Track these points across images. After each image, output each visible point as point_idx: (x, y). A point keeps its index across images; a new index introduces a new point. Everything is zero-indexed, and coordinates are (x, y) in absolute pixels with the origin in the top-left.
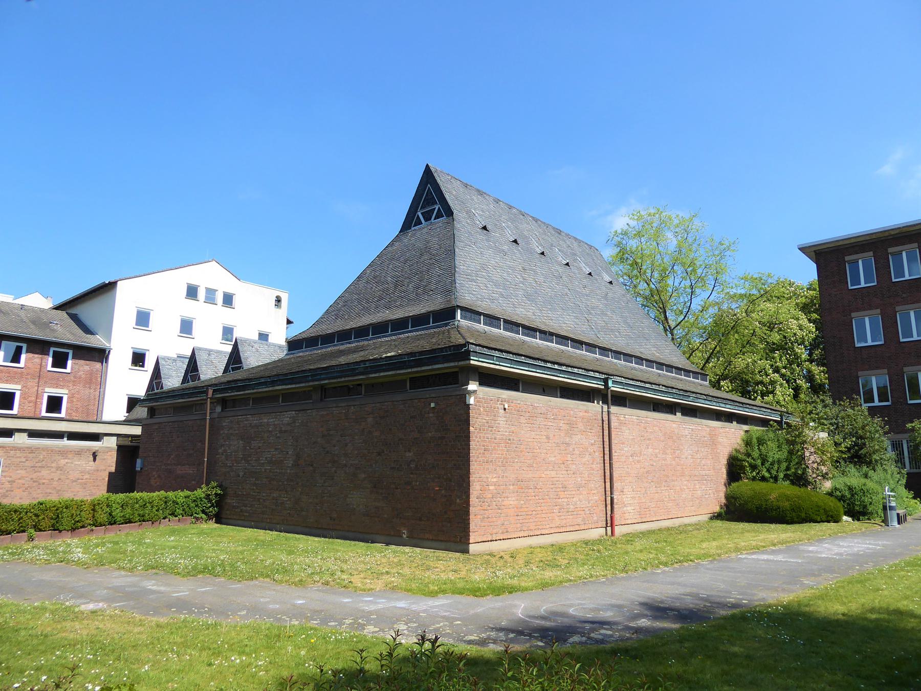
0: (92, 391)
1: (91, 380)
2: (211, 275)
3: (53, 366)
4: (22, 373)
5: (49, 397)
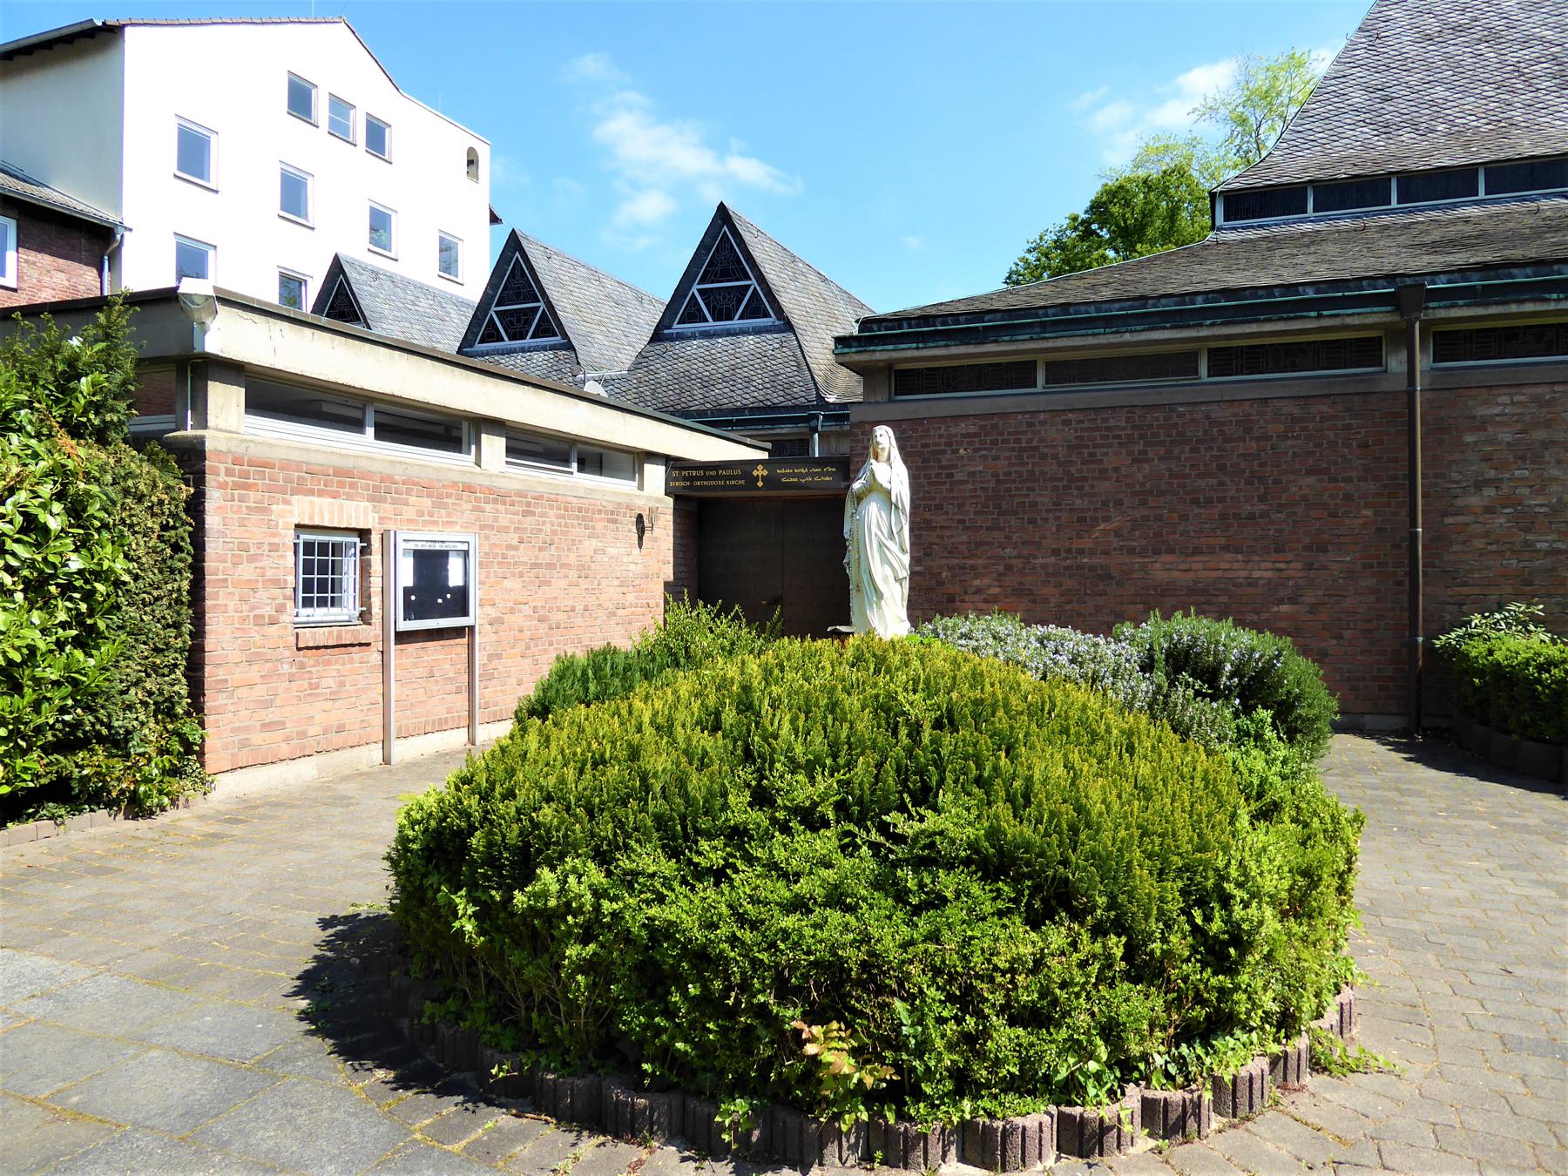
2: (334, 58)
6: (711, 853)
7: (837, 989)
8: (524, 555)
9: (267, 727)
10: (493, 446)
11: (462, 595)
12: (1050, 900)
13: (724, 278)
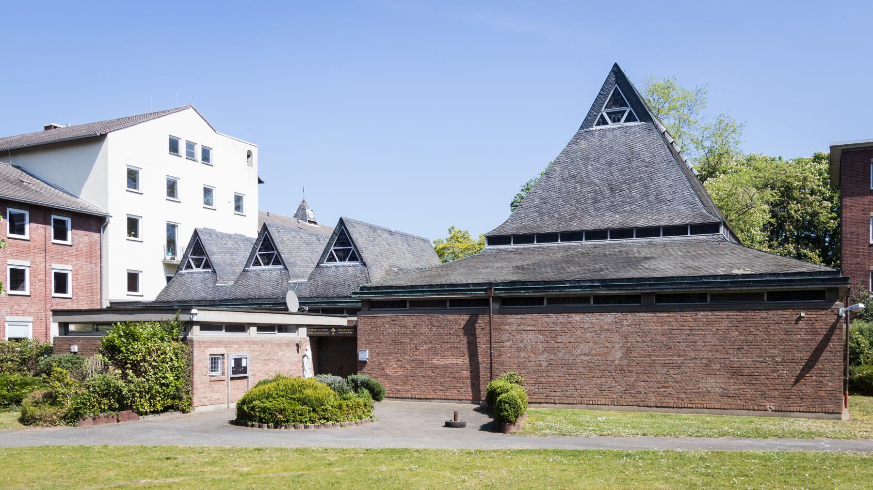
0: (93, 266)
1: (91, 253)
3: (55, 238)
4: (29, 246)
5: (55, 273)
6: (271, 399)
7: (282, 411)
8: (262, 357)
9: (205, 398)
10: (253, 330)
11: (245, 368)
12: (304, 404)
13: (343, 244)
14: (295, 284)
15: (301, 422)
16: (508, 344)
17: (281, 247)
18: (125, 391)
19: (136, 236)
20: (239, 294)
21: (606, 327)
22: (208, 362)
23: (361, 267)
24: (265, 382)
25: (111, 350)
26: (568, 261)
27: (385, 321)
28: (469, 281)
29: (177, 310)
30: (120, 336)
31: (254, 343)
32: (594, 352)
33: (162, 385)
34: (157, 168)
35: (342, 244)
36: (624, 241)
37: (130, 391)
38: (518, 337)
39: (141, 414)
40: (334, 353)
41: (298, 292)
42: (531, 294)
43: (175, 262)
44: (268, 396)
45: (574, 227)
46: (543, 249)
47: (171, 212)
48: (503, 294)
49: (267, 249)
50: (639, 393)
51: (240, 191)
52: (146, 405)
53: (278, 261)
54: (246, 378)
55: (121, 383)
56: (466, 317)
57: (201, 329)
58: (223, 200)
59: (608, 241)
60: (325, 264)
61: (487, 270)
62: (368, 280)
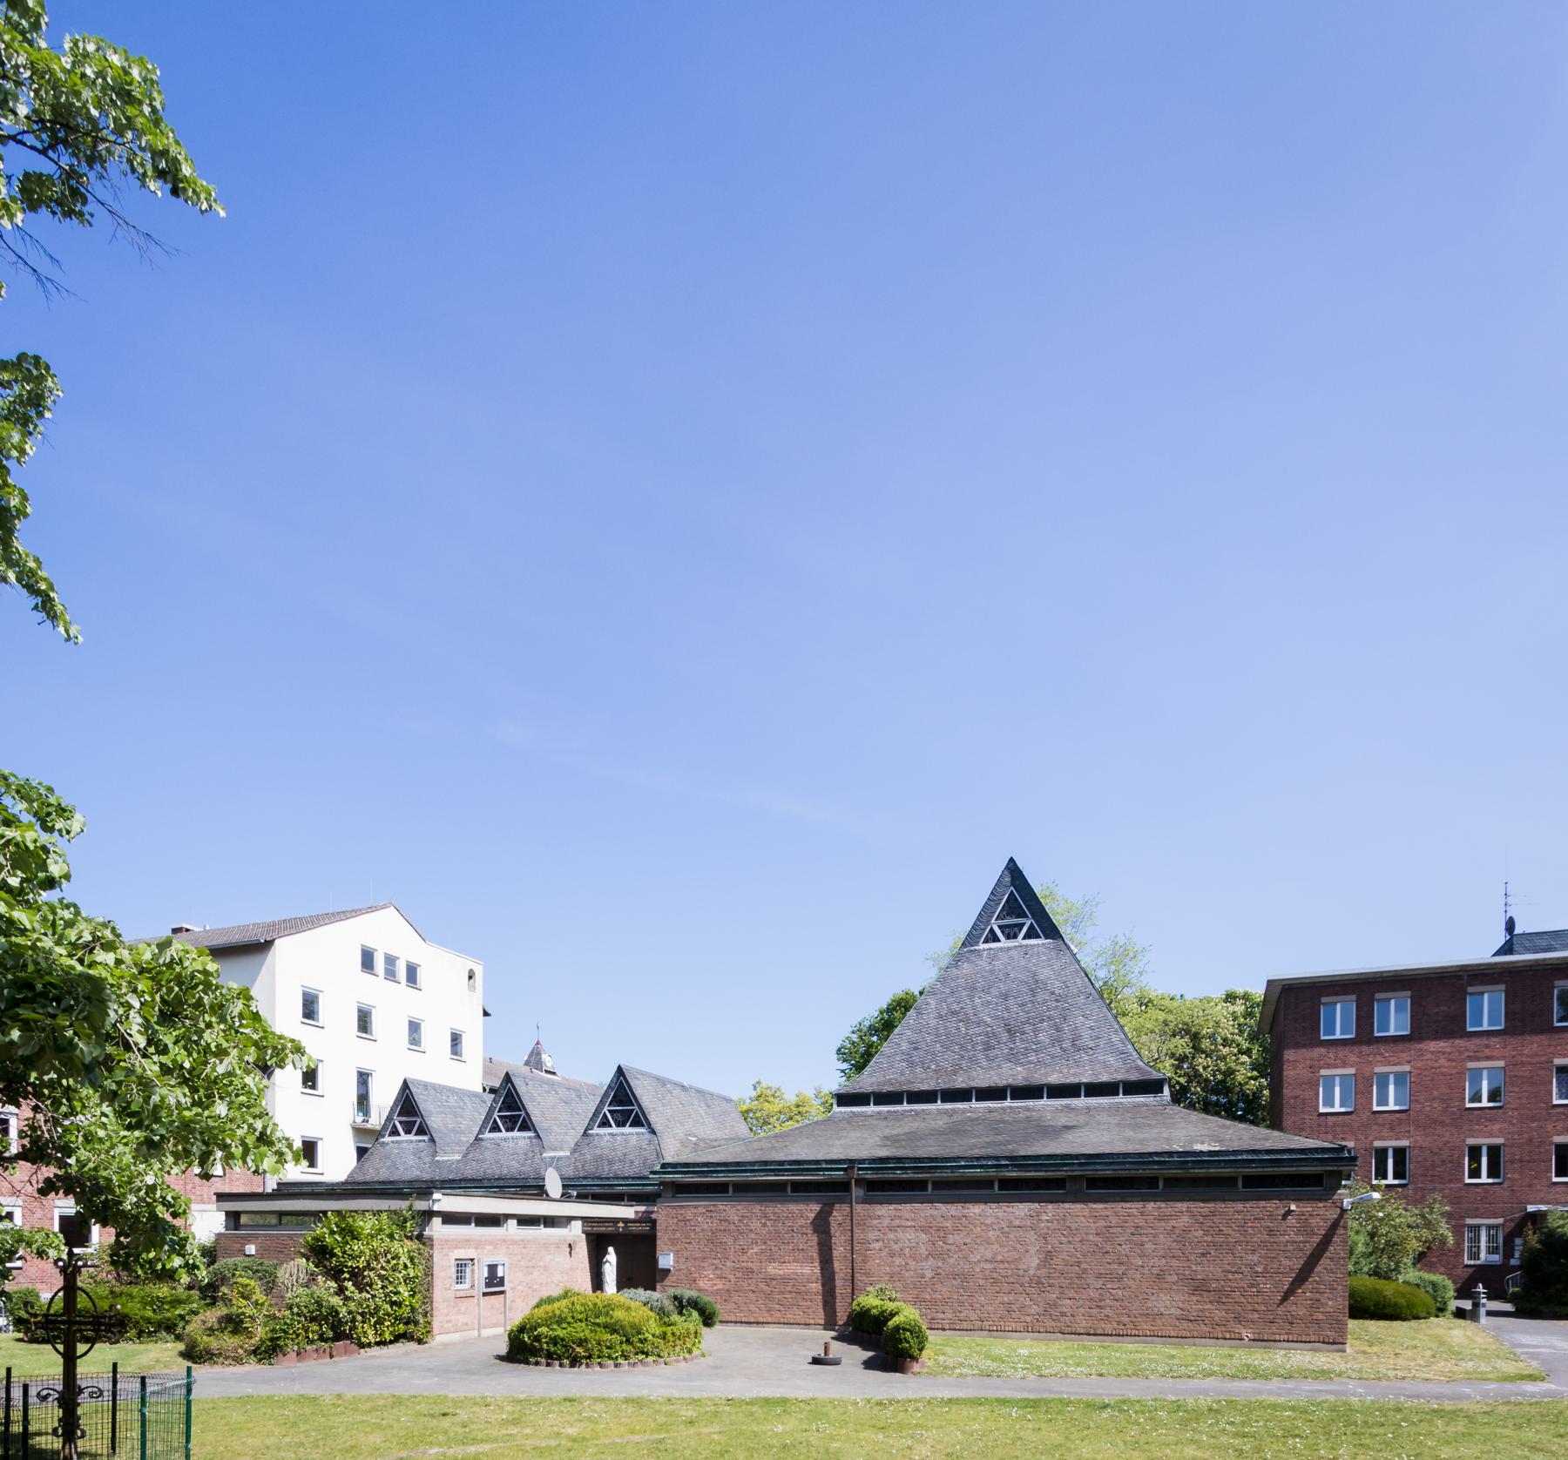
7: (581, 1342)
10: (512, 1223)
11: (502, 1279)
12: (614, 1331)
13: (622, 1102)
14: (552, 1158)
15: (610, 1357)
16: (877, 1245)
17: (529, 1106)
18: (343, 1312)
19: (313, 1087)
20: (469, 1172)
21: (1017, 1223)
22: (454, 1270)
23: (648, 1136)
24: (550, 1300)
25: (319, 1252)
26: (955, 1130)
27: (697, 1211)
28: (820, 1157)
29: (410, 1194)
30: (332, 1233)
31: (514, 1243)
32: (999, 1258)
33: (393, 1303)
34: (344, 992)
35: (620, 1103)
36: (1030, 1103)
37: (350, 1312)
38: (891, 1236)
39: (362, 1346)
40: (636, 1256)
41: (557, 1169)
42: (910, 1175)
43: (369, 1126)
44: (560, 1321)
45: (960, 1082)
46: (917, 1113)
47: (363, 1054)
48: (870, 1175)
49: (509, 1106)
50: (1063, 1314)
51: (459, 1027)
52: (371, 1332)
53: (526, 1125)
54: (502, 1292)
55: (336, 1301)
56: (816, 1207)
57: (444, 1222)
58: (436, 1039)
59: (1008, 1103)
60: (596, 1130)
61: (842, 1142)
62: (659, 1154)
